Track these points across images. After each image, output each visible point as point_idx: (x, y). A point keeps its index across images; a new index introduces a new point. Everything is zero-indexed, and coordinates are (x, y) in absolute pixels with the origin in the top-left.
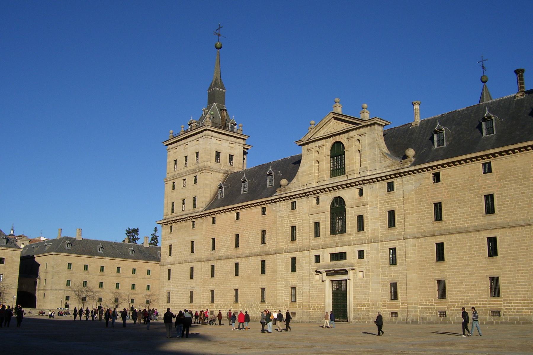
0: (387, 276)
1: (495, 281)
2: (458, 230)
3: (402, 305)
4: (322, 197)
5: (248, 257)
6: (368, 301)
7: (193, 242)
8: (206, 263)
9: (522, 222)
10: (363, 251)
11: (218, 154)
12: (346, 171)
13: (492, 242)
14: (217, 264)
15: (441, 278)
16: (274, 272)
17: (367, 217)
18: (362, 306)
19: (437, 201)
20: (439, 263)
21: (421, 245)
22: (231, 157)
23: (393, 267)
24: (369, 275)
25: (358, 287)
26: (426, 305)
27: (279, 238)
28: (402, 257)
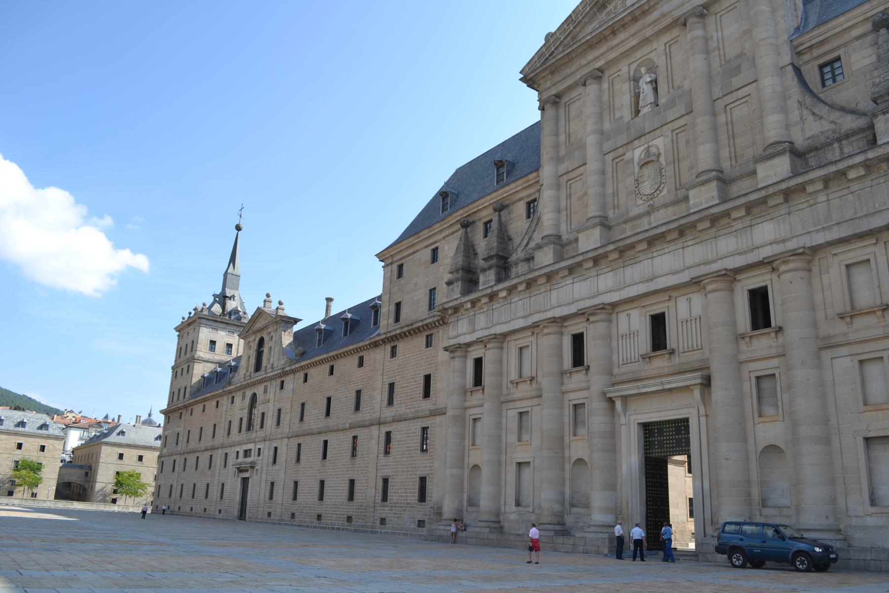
9: (341, 426)
11: (213, 343)
15: (296, 479)
19: (303, 401)
22: (229, 346)
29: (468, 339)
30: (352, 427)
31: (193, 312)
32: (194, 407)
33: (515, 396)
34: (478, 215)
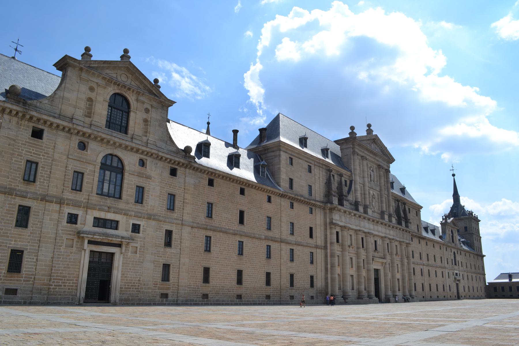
0: (161, 257)
2: (223, 230)
3: (173, 287)
4: (92, 145)
6: (139, 280)
15: (207, 266)
17: (148, 191)
18: (132, 286)
20: (206, 253)
21: (195, 234)
23: (168, 249)
24: (143, 252)
25: (129, 264)
26: (194, 288)
28: (178, 241)
30: (267, 238)
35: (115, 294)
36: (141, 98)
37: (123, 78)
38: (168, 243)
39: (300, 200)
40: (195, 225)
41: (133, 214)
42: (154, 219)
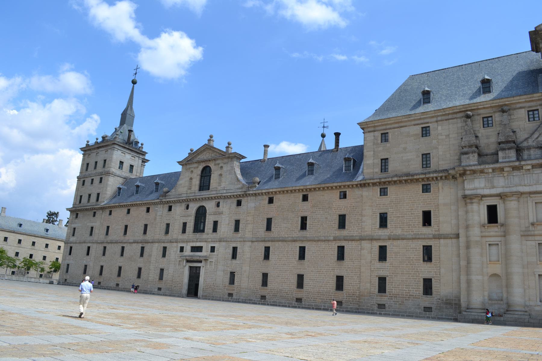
1: (301, 278)
2: (281, 239)
5: (132, 243)
7: (92, 228)
8: (100, 245)
10: (214, 247)
11: (122, 163)
12: (211, 187)
13: (302, 250)
14: (108, 247)
15: (265, 272)
16: (150, 256)
19: (269, 217)
22: (132, 166)
23: (234, 261)
27: (156, 232)
29: (487, 192)
30: (335, 239)
31: (100, 140)
32: (113, 210)
33: (536, 233)
34: (476, 111)
35: (200, 293)
36: (218, 162)
37: (205, 156)
38: (234, 256)
39: (395, 182)
40: (254, 239)
41: (210, 240)
42: (223, 241)
